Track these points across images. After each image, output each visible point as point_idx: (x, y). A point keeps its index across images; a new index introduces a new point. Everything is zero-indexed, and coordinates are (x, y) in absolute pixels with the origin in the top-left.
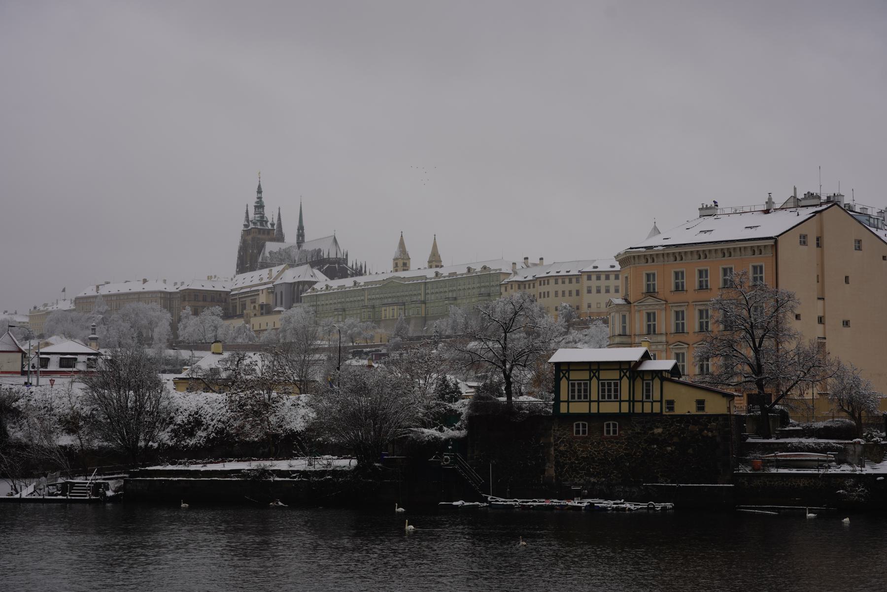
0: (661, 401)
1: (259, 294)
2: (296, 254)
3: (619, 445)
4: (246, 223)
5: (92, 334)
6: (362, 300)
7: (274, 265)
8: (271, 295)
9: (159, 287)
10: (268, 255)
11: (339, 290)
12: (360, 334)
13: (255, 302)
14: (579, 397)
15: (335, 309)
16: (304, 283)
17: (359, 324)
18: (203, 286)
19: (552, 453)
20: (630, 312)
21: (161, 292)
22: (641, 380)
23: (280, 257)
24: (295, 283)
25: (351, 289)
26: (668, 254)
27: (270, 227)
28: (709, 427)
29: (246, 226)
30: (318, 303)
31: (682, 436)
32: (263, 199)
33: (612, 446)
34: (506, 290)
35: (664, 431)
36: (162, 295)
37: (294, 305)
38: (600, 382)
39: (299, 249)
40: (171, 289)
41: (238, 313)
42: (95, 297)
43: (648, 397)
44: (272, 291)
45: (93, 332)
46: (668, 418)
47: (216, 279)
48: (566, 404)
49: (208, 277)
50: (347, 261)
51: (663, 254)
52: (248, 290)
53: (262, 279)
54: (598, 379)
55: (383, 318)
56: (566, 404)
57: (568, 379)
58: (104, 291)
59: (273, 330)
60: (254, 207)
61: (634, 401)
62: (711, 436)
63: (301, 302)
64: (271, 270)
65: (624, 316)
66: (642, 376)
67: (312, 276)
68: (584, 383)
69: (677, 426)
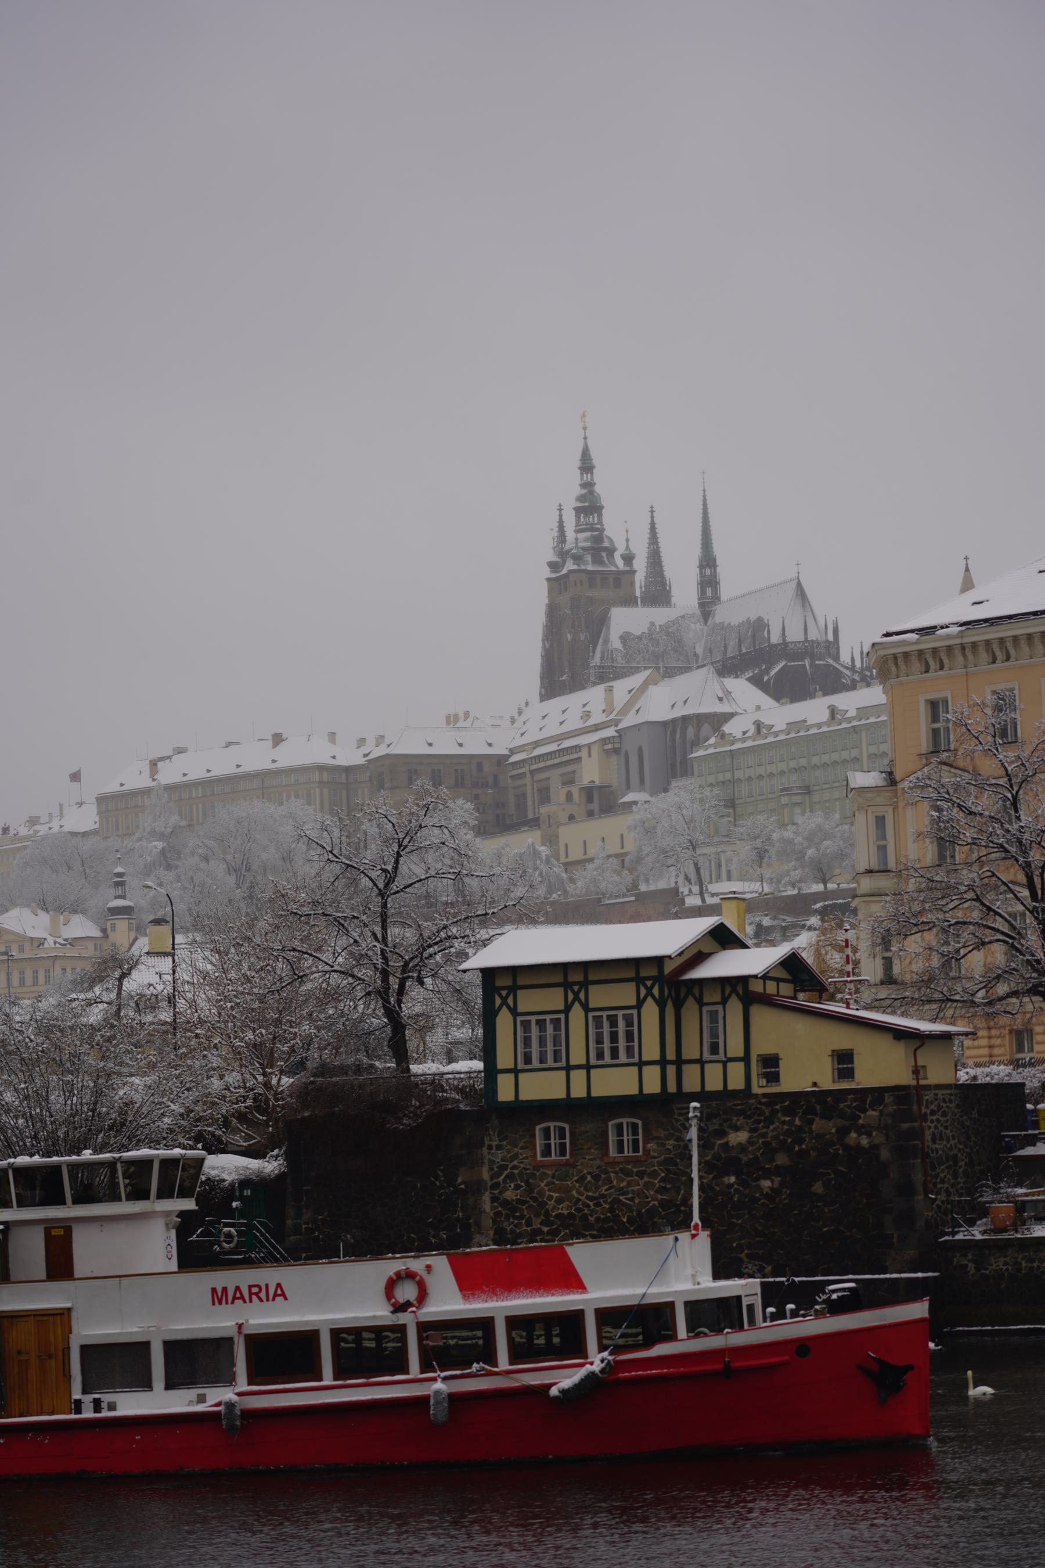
0: (746, 1059)
1: (579, 759)
2: (697, 637)
3: (646, 1179)
4: (556, 559)
5: (117, 897)
7: (619, 674)
8: (614, 759)
9: (320, 753)
10: (616, 643)
11: (792, 735)
12: (841, 856)
13: (572, 782)
15: (782, 790)
16: (700, 719)
17: (840, 828)
18: (430, 745)
19: (487, 1205)
20: (895, 808)
21: (321, 768)
22: (697, 1007)
23: (651, 648)
24: (674, 721)
25: (824, 729)
26: (974, 645)
27: (620, 564)
28: (861, 1122)
29: (553, 566)
30: (738, 774)
31: (797, 1149)
32: (597, 489)
33: (629, 1184)
35: (750, 1138)
36: (325, 777)
37: (673, 784)
38: (591, 1015)
39: (706, 624)
40: (349, 756)
42: (146, 792)
43: (714, 1049)
44: (613, 748)
45: (120, 893)
46: (760, 1103)
47: (468, 723)
48: (511, 1076)
49: (448, 717)
50: (838, 648)
51: (963, 647)
52: (553, 747)
53: (587, 715)
54: (586, 1008)
57: (514, 1012)
58: (170, 774)
59: (611, 859)
60: (573, 513)
61: (680, 1062)
62: (867, 1146)
63: (693, 774)
64: (610, 690)
65: (880, 821)
66: (697, 994)
67: (721, 699)
68: (551, 1020)
69: (784, 1123)
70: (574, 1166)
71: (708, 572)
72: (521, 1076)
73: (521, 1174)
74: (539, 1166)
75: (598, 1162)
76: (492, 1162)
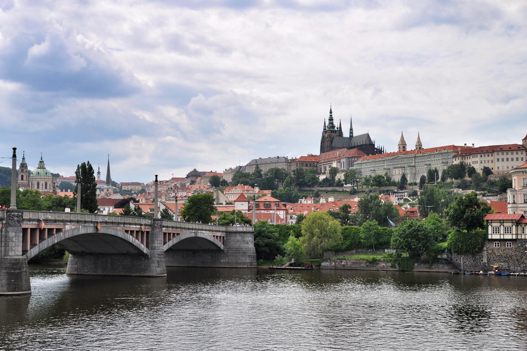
6: (384, 166)
8: (339, 163)
14: (496, 233)
34: (455, 160)
41: (322, 172)
54: (503, 226)
57: (492, 226)
61: (518, 234)
65: (514, 196)
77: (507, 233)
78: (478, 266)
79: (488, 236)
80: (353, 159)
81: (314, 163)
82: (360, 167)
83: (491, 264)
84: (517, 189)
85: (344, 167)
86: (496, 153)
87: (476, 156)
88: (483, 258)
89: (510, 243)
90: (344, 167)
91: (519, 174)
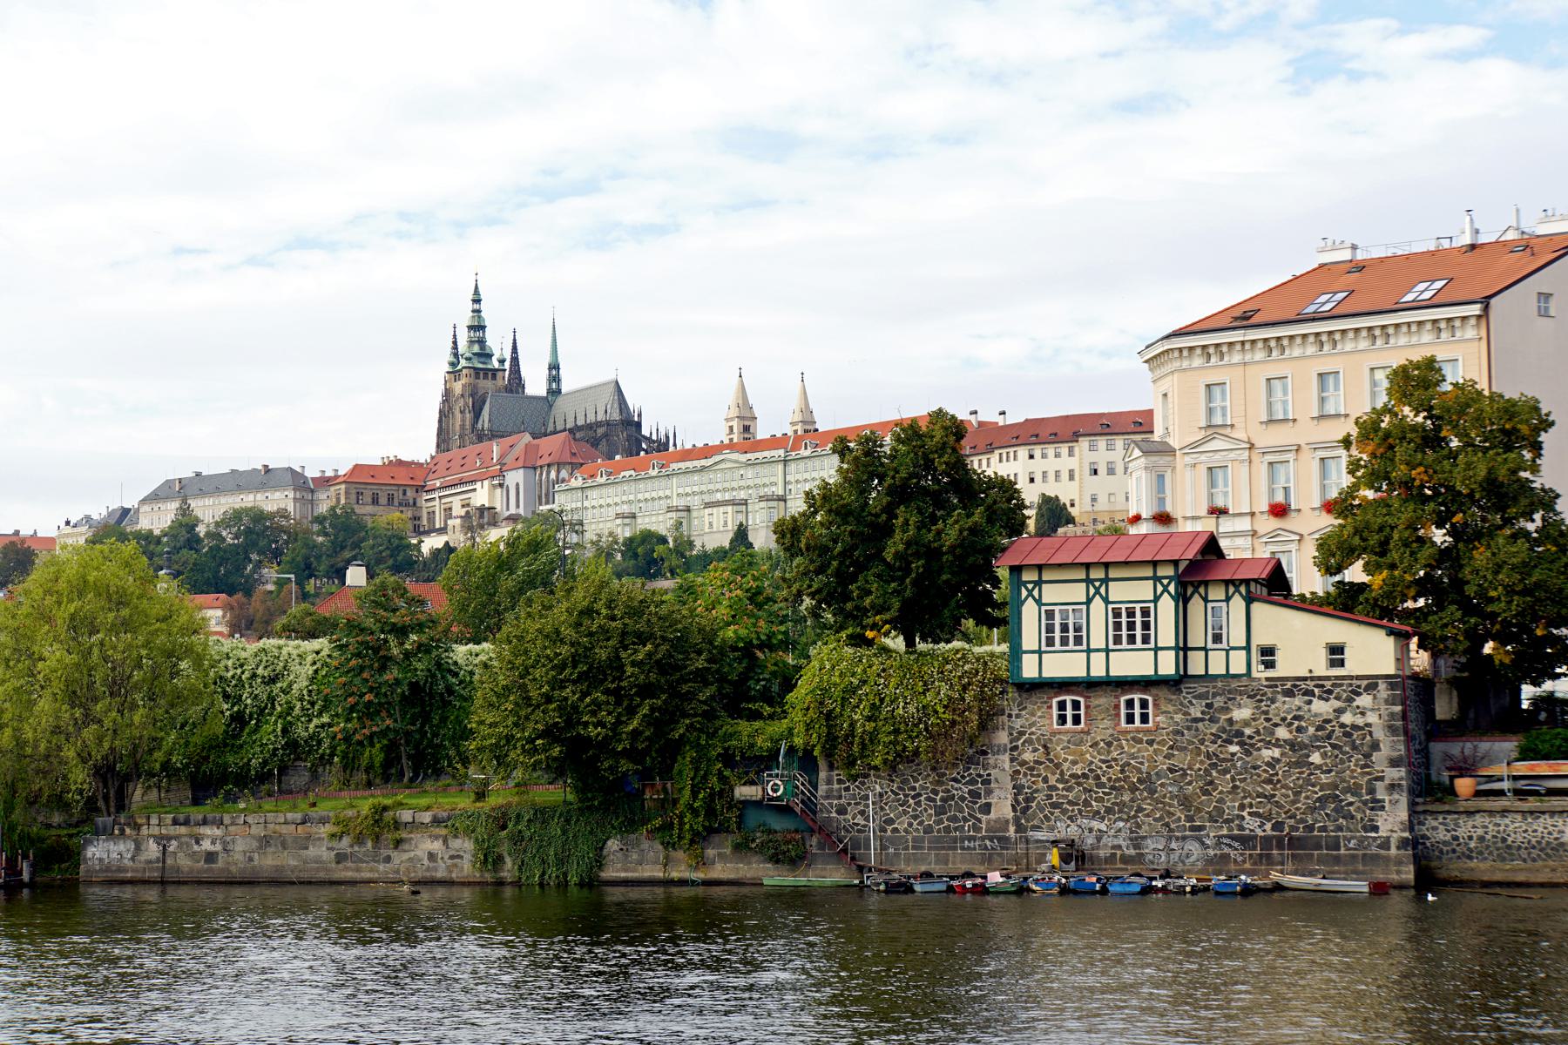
0: (1248, 648)
3: (1155, 746)
8: (499, 490)
22: (1202, 603)
29: (452, 364)
30: (586, 504)
33: (1139, 750)
38: (1110, 607)
41: (437, 526)
48: (1036, 656)
54: (1106, 601)
55: (707, 530)
56: (1036, 656)
57: (1039, 602)
70: (1088, 733)
71: (554, 372)
72: (1044, 656)
73: (1038, 739)
74: (1054, 734)
75: (1110, 731)
76: (1011, 728)
77: (1125, 645)
78: (963, 840)
79: (1020, 660)
80: (553, 475)
81: (404, 494)
82: (579, 504)
83: (1036, 828)
84: (1174, 442)
85: (518, 506)
86: (1084, 443)
87: (1012, 455)
88: (989, 792)
89: (1144, 704)
90: (518, 506)
91: (1185, 364)
